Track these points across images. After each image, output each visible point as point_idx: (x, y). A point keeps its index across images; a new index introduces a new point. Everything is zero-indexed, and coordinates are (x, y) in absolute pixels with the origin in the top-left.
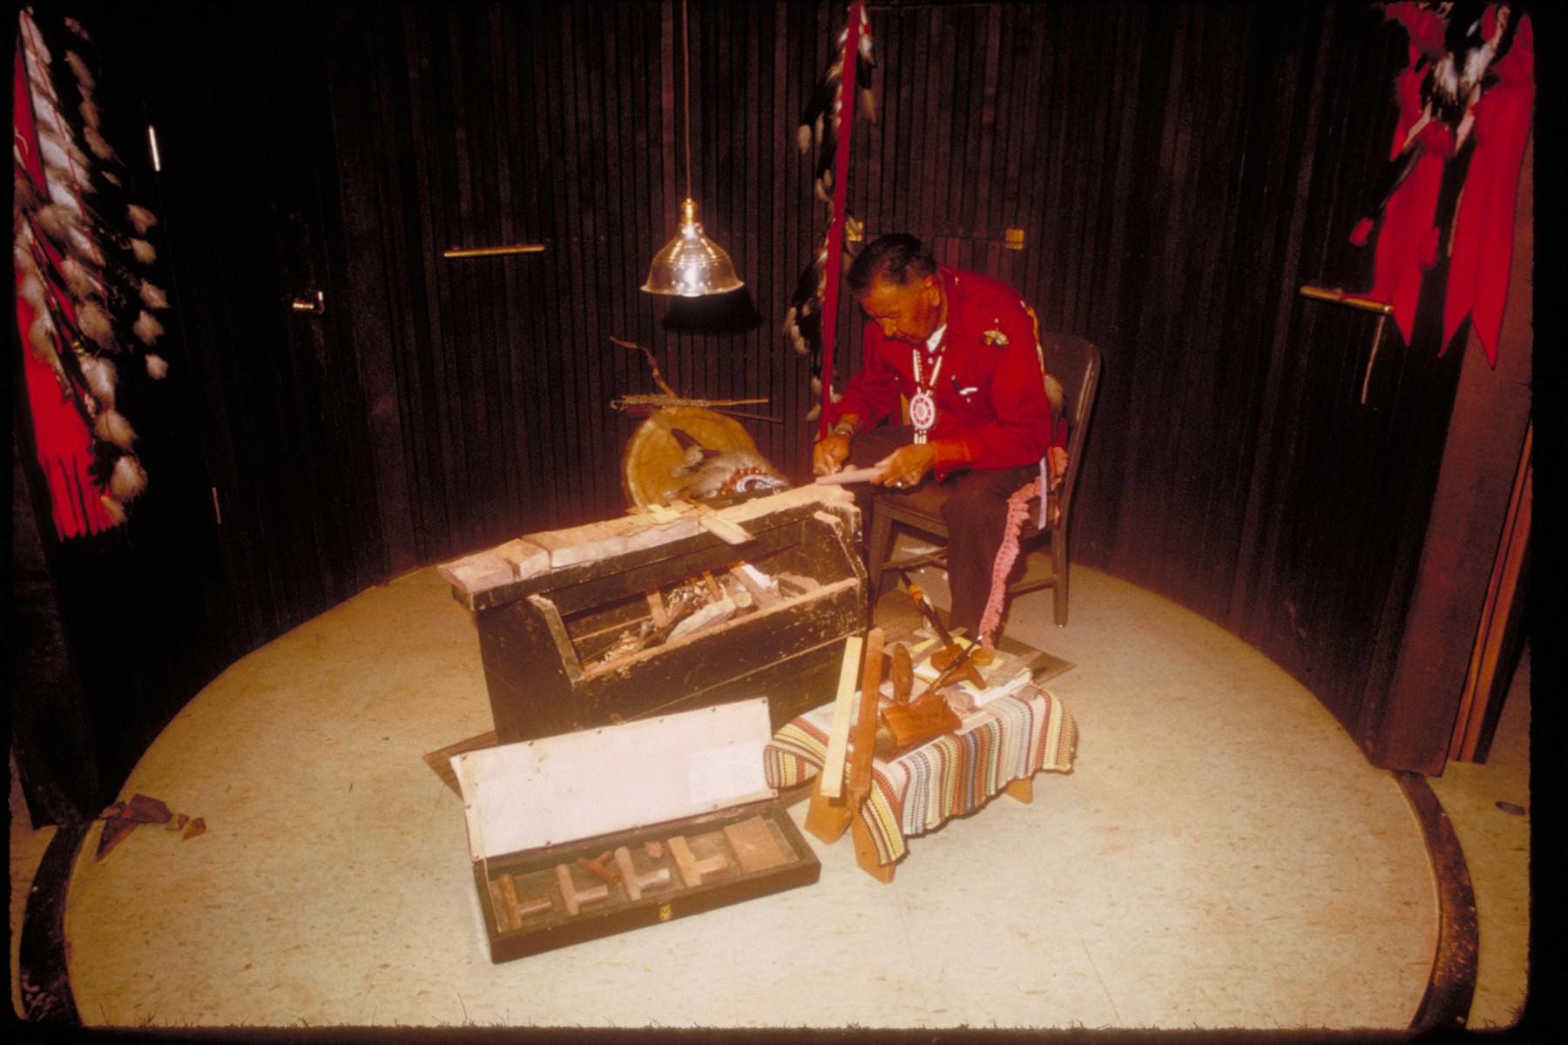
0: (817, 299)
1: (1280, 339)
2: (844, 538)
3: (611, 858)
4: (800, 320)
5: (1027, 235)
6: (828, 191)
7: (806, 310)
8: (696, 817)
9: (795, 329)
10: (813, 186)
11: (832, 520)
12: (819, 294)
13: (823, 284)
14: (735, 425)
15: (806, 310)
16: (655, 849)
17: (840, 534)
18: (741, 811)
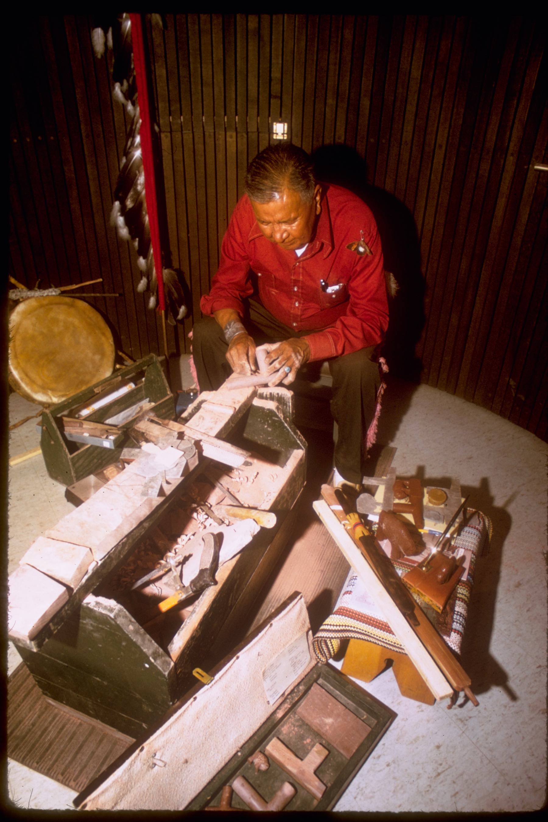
0: (138, 194)
1: (502, 202)
2: (284, 418)
3: (232, 792)
4: (123, 211)
5: (290, 129)
6: (129, 95)
7: (129, 204)
8: (274, 713)
9: (121, 220)
10: (111, 89)
11: (271, 405)
12: (139, 188)
13: (141, 180)
14: (81, 304)
15: (129, 204)
16: (259, 761)
17: (281, 416)
18: (301, 688)
